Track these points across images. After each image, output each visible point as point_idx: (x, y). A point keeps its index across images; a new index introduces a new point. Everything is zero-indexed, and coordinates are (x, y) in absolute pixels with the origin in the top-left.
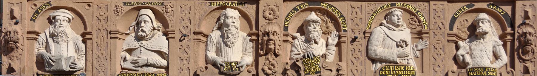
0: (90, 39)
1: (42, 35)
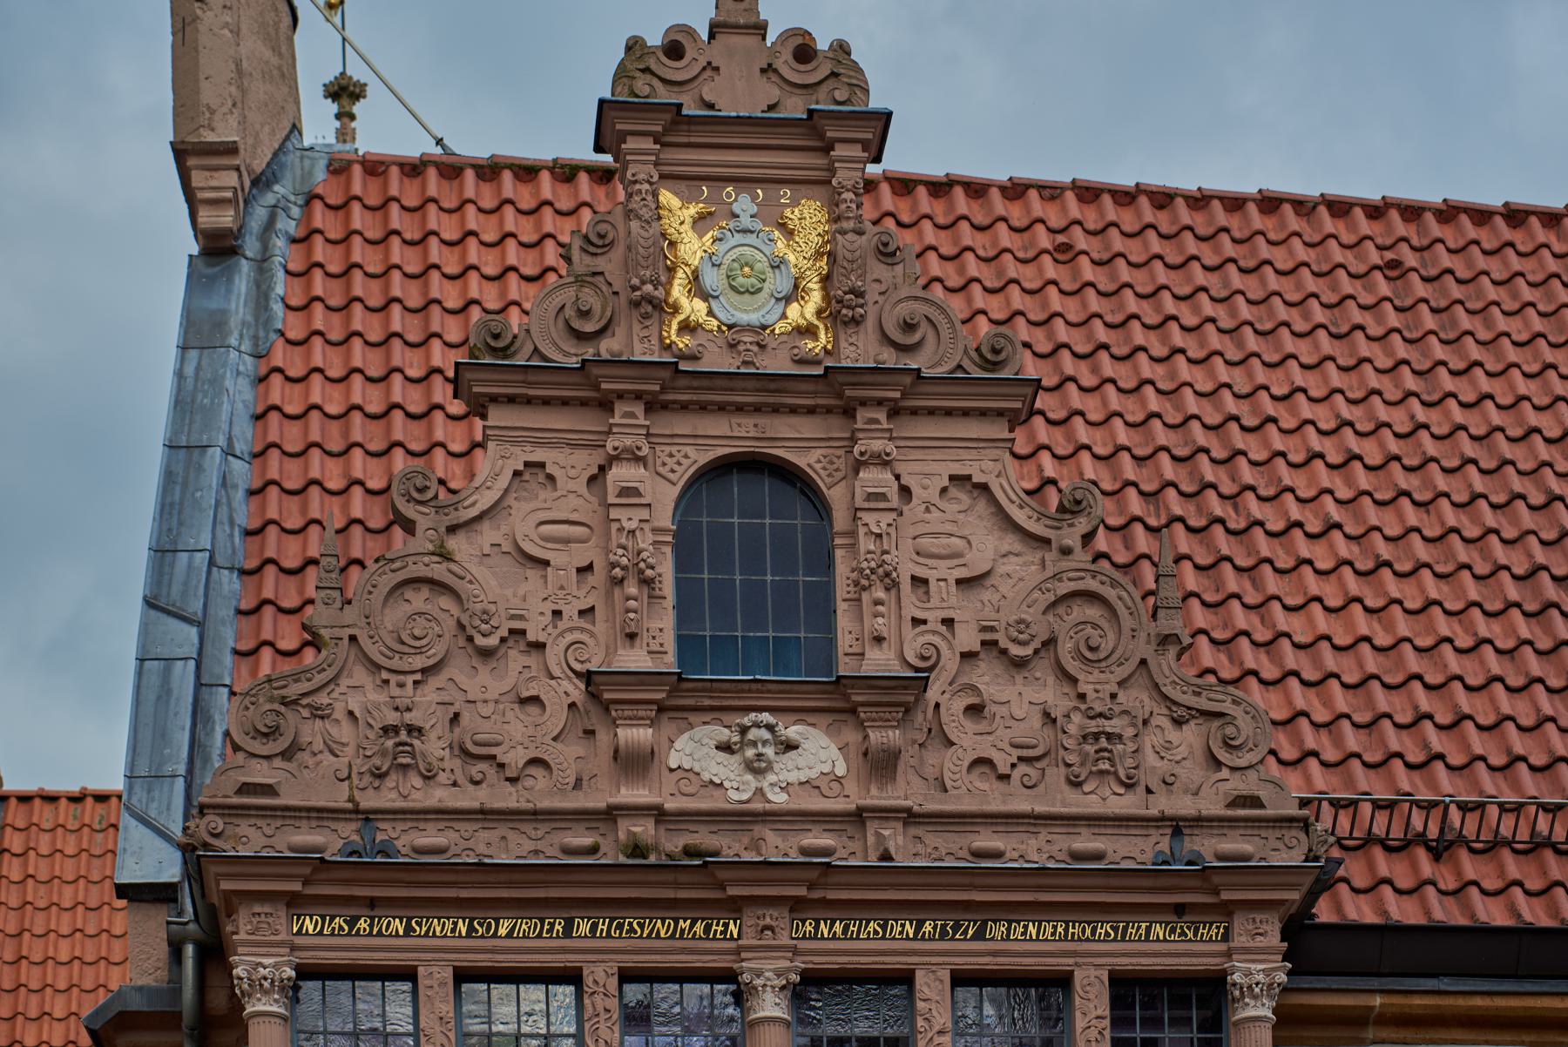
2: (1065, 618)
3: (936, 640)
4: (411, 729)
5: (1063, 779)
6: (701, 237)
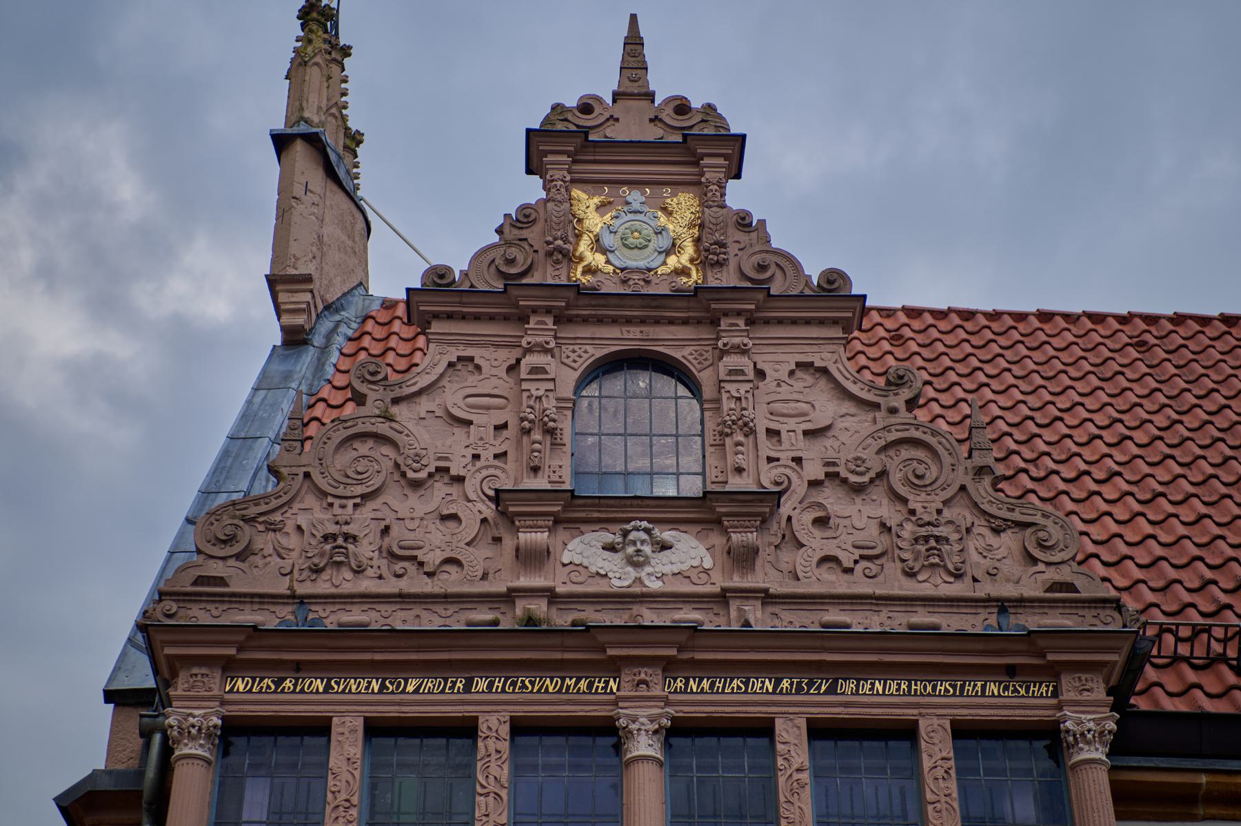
2: (895, 458)
3: (788, 471)
4: (347, 537)
5: (899, 572)
6: (602, 216)
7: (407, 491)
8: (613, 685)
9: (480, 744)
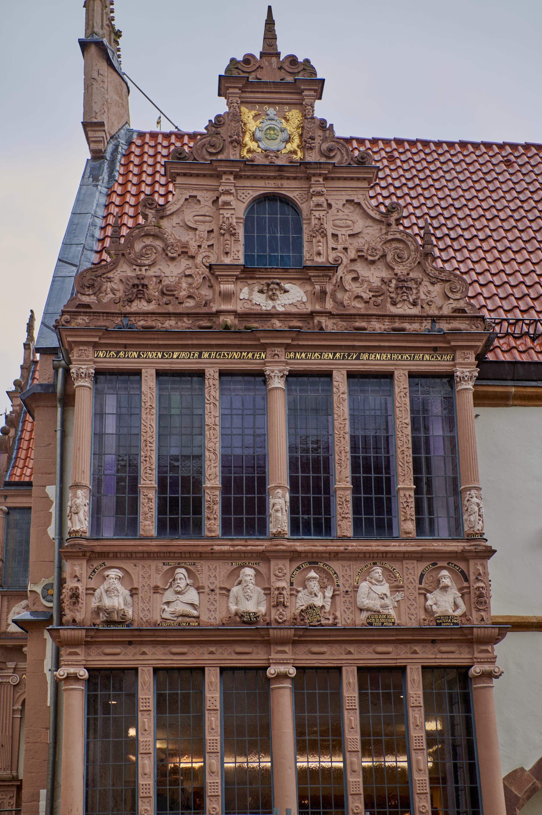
0: (136, 594)
1: (98, 591)
4: (144, 286)
6: (256, 121)
7: (169, 263)
8: (263, 355)
9: (206, 382)
